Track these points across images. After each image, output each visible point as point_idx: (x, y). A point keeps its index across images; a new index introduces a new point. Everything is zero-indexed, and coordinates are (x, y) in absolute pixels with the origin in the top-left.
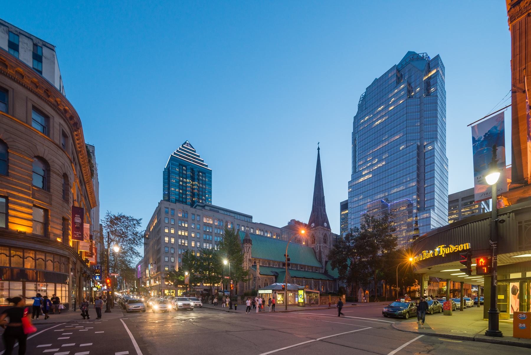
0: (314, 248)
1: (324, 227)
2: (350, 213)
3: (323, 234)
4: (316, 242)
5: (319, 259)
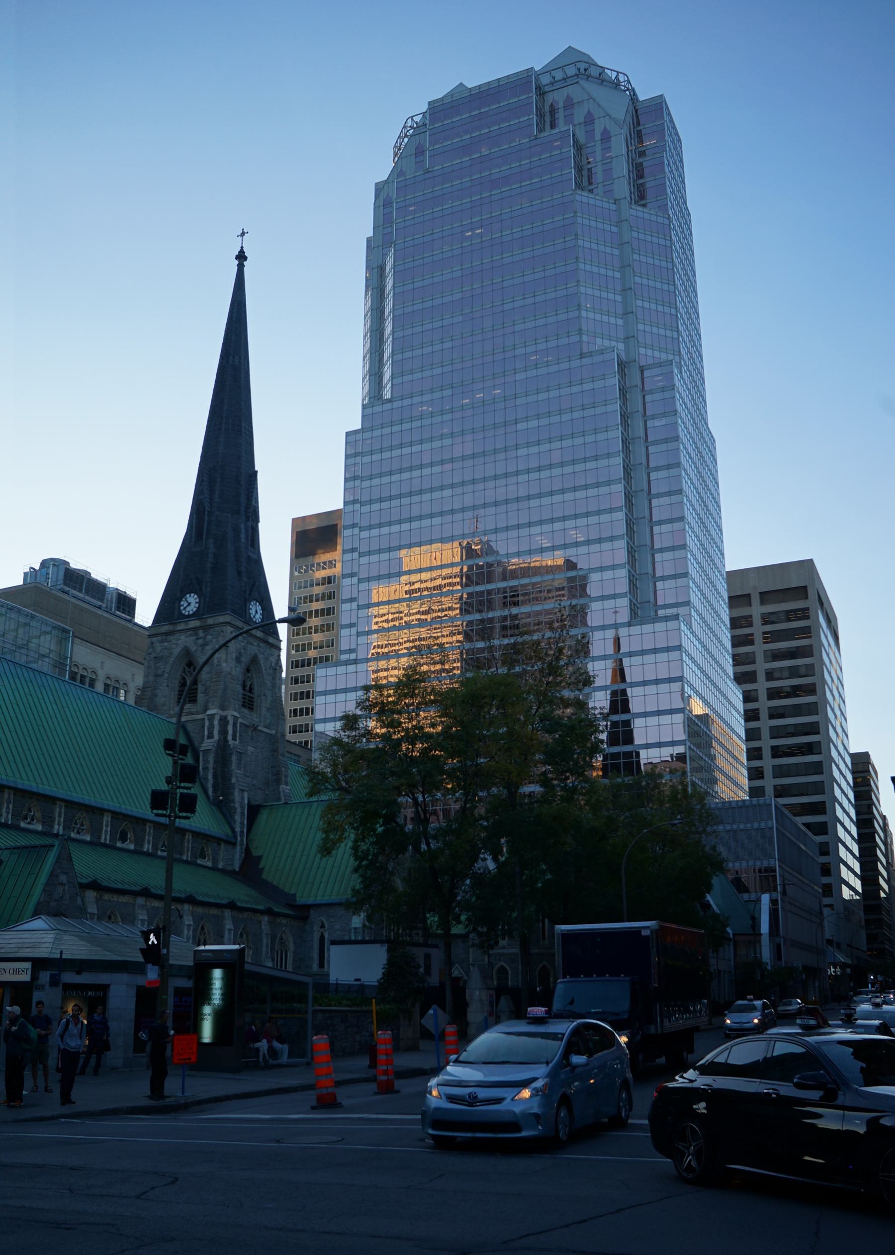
0: (190, 727)
1: (248, 620)
2: (352, 575)
3: (245, 660)
4: (200, 696)
5: (215, 791)
